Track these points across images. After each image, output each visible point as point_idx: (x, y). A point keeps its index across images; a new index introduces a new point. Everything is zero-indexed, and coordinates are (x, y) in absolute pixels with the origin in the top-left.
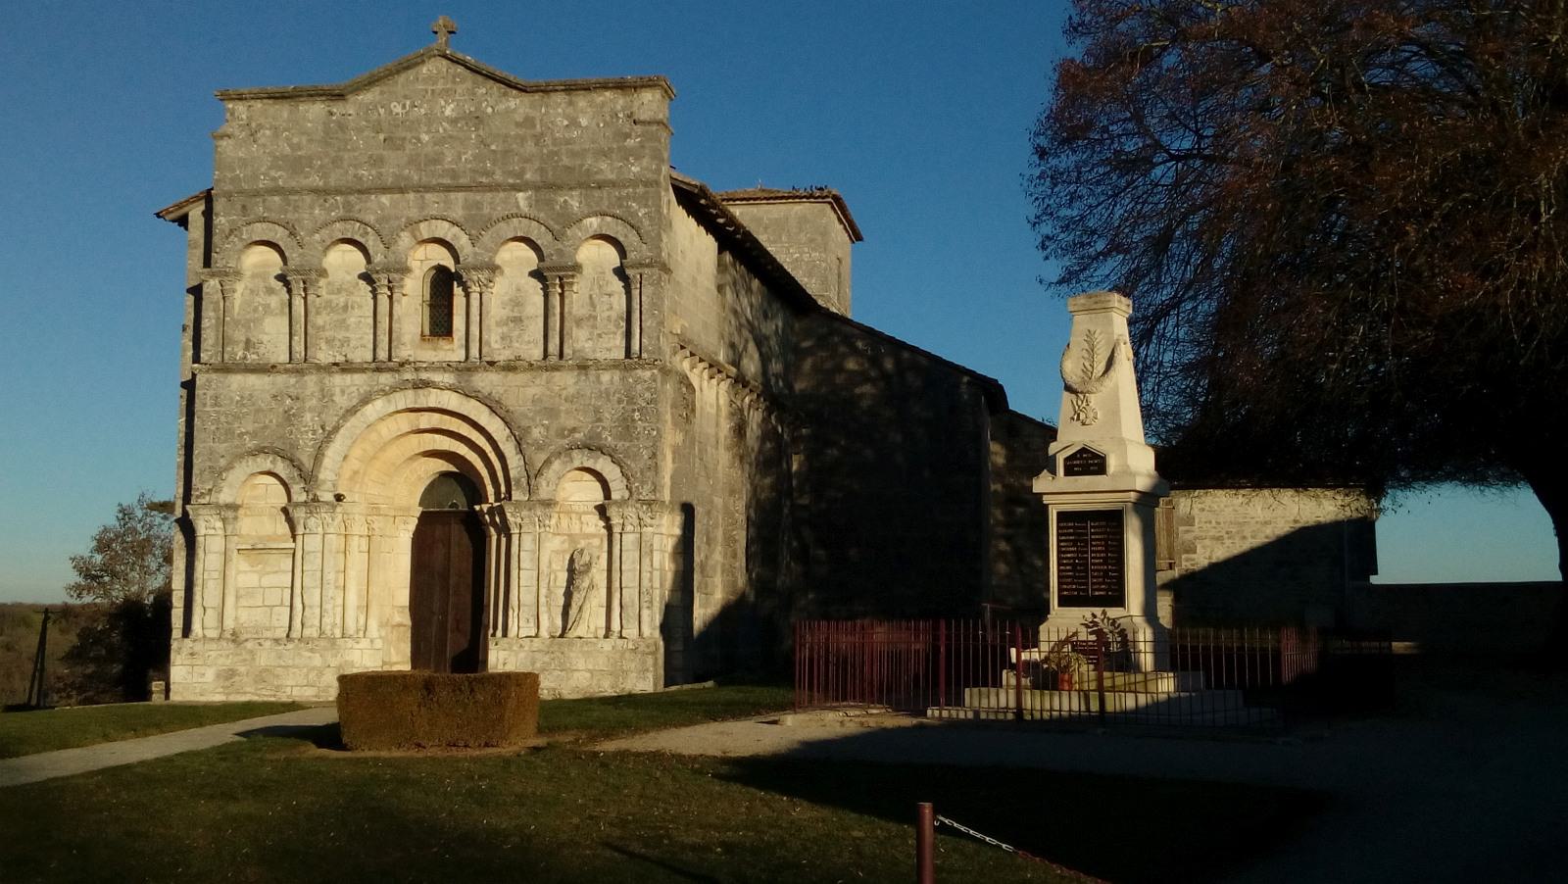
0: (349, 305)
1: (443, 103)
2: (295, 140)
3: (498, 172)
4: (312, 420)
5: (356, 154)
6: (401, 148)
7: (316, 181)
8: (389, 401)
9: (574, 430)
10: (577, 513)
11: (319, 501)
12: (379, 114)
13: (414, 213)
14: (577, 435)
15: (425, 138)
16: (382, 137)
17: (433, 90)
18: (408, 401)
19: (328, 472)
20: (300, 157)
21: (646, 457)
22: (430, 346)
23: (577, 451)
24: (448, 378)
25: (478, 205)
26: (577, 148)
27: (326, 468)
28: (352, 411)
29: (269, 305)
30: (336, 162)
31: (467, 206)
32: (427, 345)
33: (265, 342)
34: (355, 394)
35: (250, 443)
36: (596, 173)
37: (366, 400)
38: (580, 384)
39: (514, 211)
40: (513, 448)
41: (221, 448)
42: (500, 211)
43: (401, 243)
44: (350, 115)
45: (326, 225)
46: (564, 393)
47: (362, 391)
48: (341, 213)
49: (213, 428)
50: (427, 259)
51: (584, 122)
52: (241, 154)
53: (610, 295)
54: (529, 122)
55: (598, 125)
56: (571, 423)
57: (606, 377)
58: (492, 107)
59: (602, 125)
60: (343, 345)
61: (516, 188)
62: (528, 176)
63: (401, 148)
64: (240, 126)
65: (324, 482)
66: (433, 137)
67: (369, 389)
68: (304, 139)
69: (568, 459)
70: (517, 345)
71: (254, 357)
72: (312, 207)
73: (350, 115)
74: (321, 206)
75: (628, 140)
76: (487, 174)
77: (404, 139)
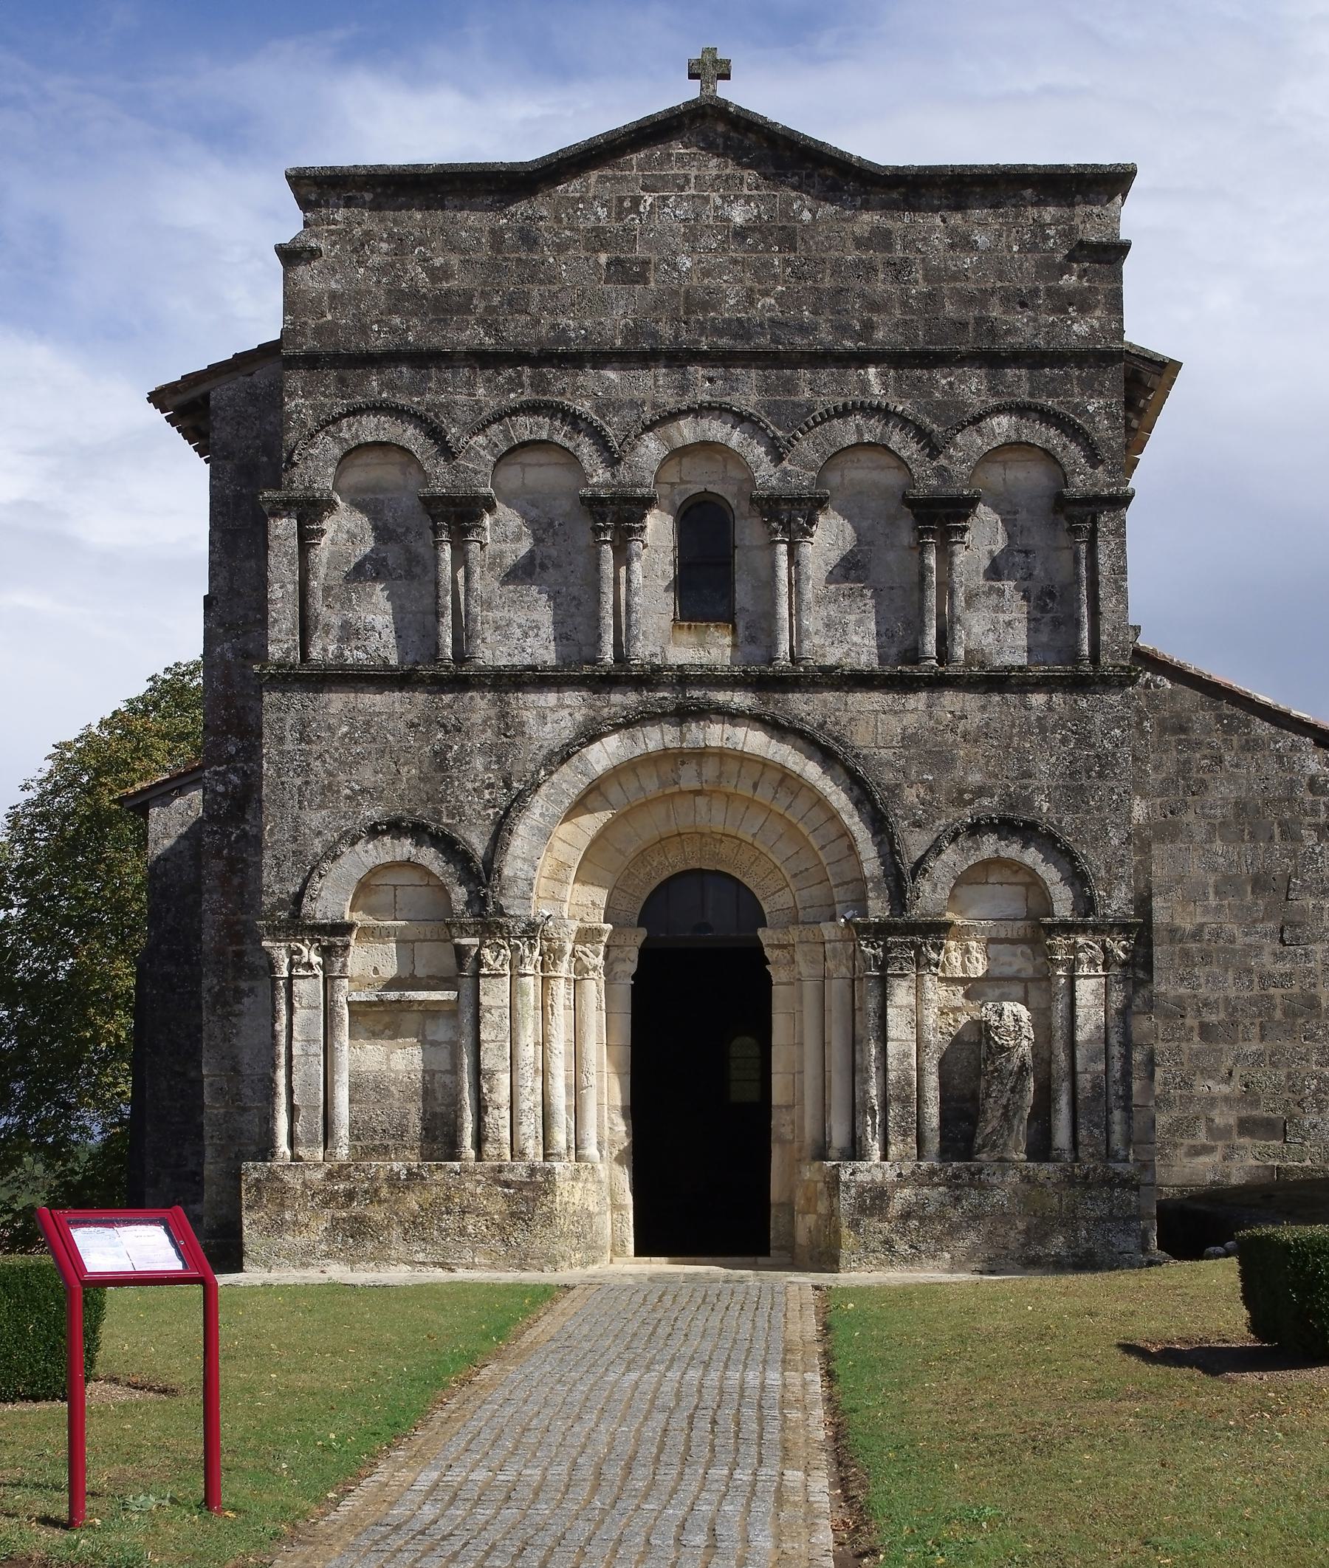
0: (538, 561)
1: (719, 201)
2: (438, 262)
3: (824, 326)
4: (487, 769)
5: (555, 288)
6: (642, 278)
7: (473, 336)
8: (633, 738)
9: (981, 792)
11: (504, 915)
12: (599, 219)
13: (669, 400)
14: (986, 802)
15: (686, 263)
16: (603, 258)
17: (696, 177)
18: (668, 738)
19: (519, 864)
20: (449, 293)
21: (1115, 842)
22: (693, 639)
24: (741, 699)
25: (790, 387)
26: (971, 286)
27: (515, 858)
28: (564, 755)
29: (385, 559)
30: (516, 303)
31: (765, 389)
32: (685, 637)
33: (379, 627)
34: (567, 722)
35: (372, 812)
36: (1008, 332)
37: (590, 735)
38: (990, 709)
39: (857, 397)
41: (314, 818)
42: (829, 400)
43: (643, 450)
44: (541, 218)
45: (498, 418)
46: (961, 726)
47: (579, 717)
48: (528, 395)
49: (298, 781)
50: (682, 482)
51: (981, 239)
52: (334, 285)
53: (1027, 553)
54: (882, 239)
55: (1010, 248)
56: (975, 778)
57: (1038, 699)
58: (810, 210)
59: (1015, 248)
60: (526, 635)
61: (862, 359)
62: (880, 335)
63: (642, 278)
64: (331, 232)
65: (514, 879)
66: (700, 262)
67: (592, 713)
68: (455, 260)
70: (856, 639)
71: (361, 655)
72: (470, 384)
73: (541, 218)
74: (489, 380)
75: (1066, 277)
76: (803, 329)
77: (646, 263)
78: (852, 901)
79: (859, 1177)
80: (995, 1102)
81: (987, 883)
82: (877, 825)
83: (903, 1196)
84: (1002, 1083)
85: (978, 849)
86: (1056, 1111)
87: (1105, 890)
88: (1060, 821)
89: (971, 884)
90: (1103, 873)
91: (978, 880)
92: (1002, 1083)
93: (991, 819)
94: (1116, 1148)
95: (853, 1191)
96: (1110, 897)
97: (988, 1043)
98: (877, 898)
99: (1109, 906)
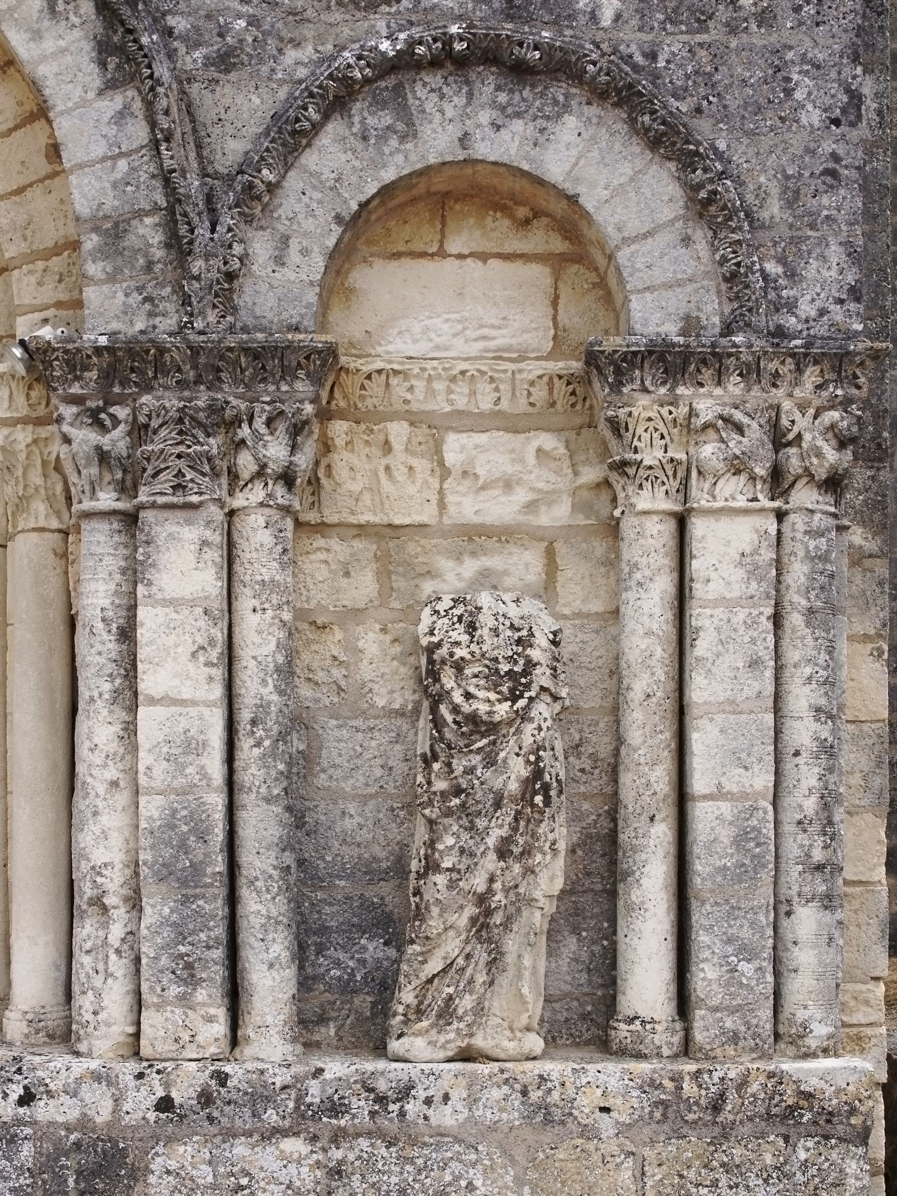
10: (414, 419)
21: (812, 116)
23: (434, 79)
40: (87, 46)
69: (387, 118)
78: (59, 305)
79: (43, 1111)
80: (452, 885)
81: (442, 253)
82: (112, 62)
83: (173, 1165)
84: (472, 828)
85: (410, 133)
86: (630, 908)
87: (782, 260)
88: (652, 56)
89: (398, 255)
90: (774, 210)
91: (418, 246)
92: (472, 828)
93: (448, 40)
94: (801, 1015)
95: (26, 1151)
96: (792, 275)
97: (434, 710)
98: (111, 278)
99: (791, 306)
